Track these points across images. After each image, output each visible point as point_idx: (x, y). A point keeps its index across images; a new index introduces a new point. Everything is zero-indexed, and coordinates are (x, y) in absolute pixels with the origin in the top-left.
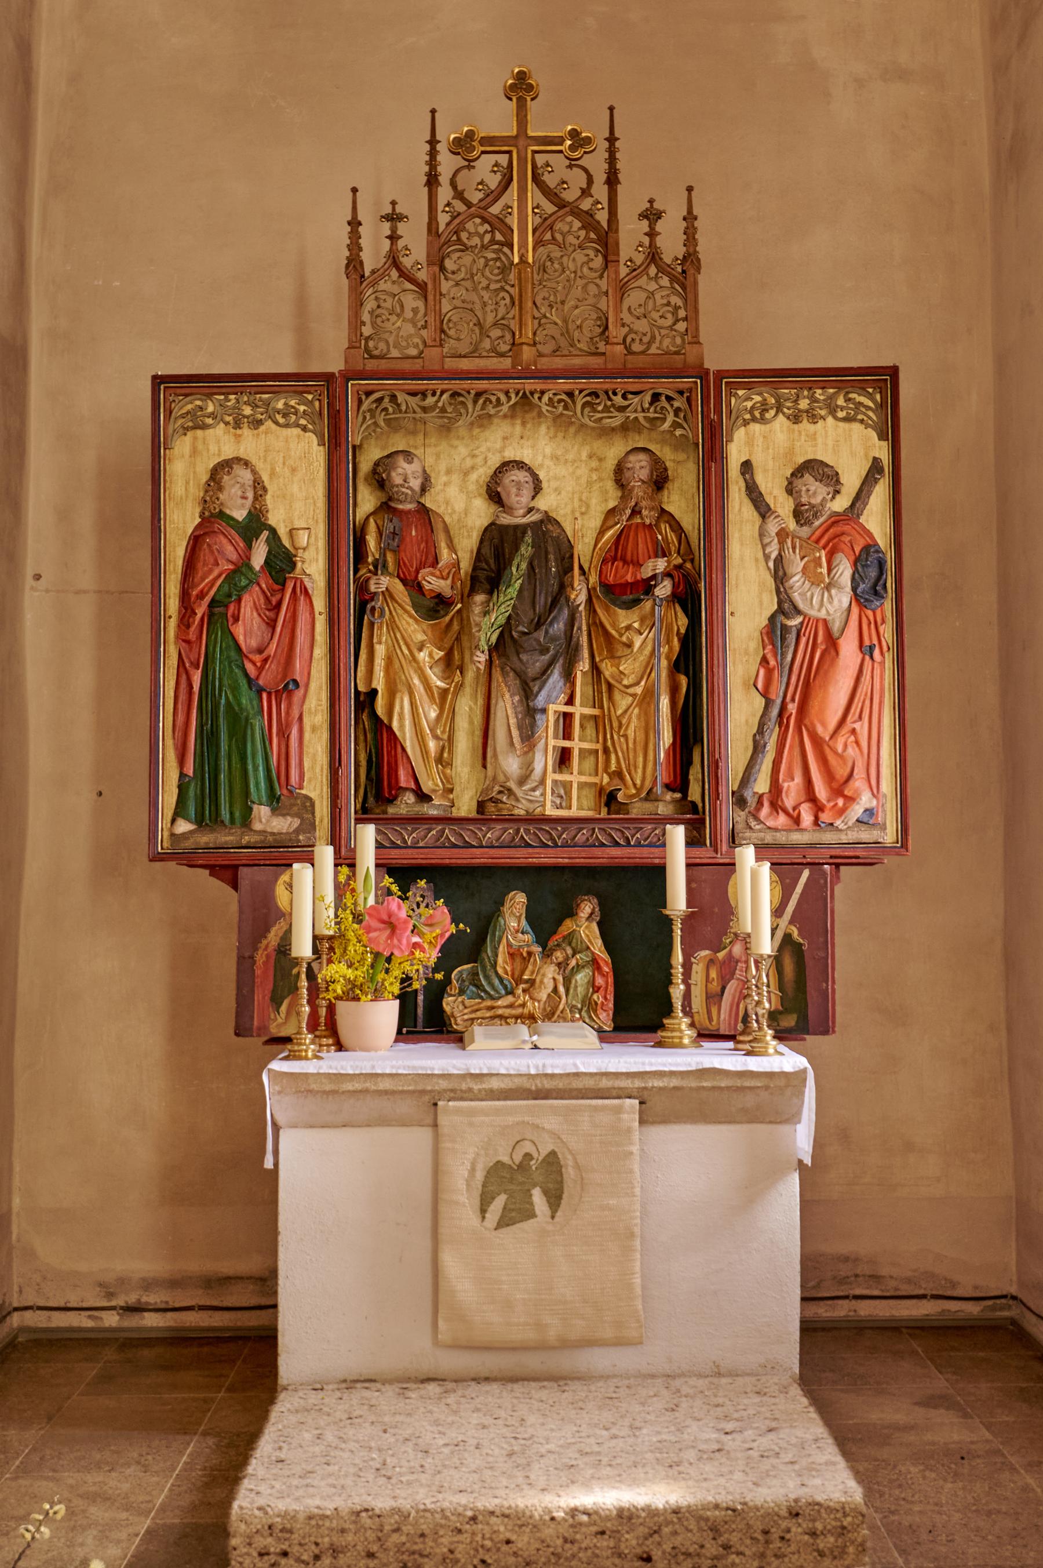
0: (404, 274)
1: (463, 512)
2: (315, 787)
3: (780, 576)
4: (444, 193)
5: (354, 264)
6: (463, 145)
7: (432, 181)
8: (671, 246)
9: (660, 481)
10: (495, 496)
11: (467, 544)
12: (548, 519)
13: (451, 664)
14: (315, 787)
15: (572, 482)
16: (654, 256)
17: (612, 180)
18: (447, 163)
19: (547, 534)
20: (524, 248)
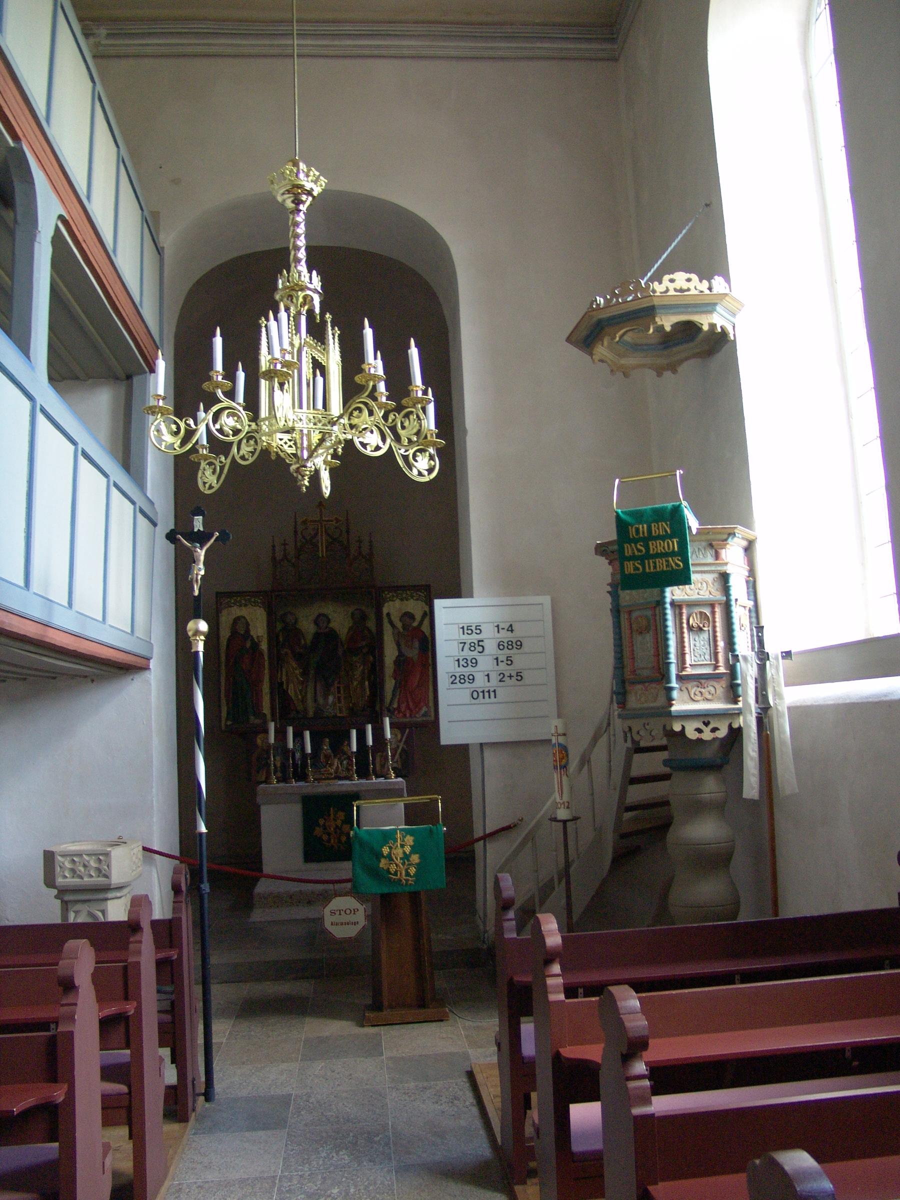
0: (289, 561)
1: (308, 627)
2: (266, 710)
3: (398, 644)
4: (300, 536)
5: (274, 558)
6: (304, 522)
7: (296, 532)
8: (365, 550)
9: (364, 617)
10: (316, 622)
11: (309, 638)
12: (332, 630)
13: (305, 673)
14: (266, 710)
15: (340, 620)
16: (360, 553)
17: (348, 532)
18: (300, 528)
19: (332, 635)
20: (322, 552)
